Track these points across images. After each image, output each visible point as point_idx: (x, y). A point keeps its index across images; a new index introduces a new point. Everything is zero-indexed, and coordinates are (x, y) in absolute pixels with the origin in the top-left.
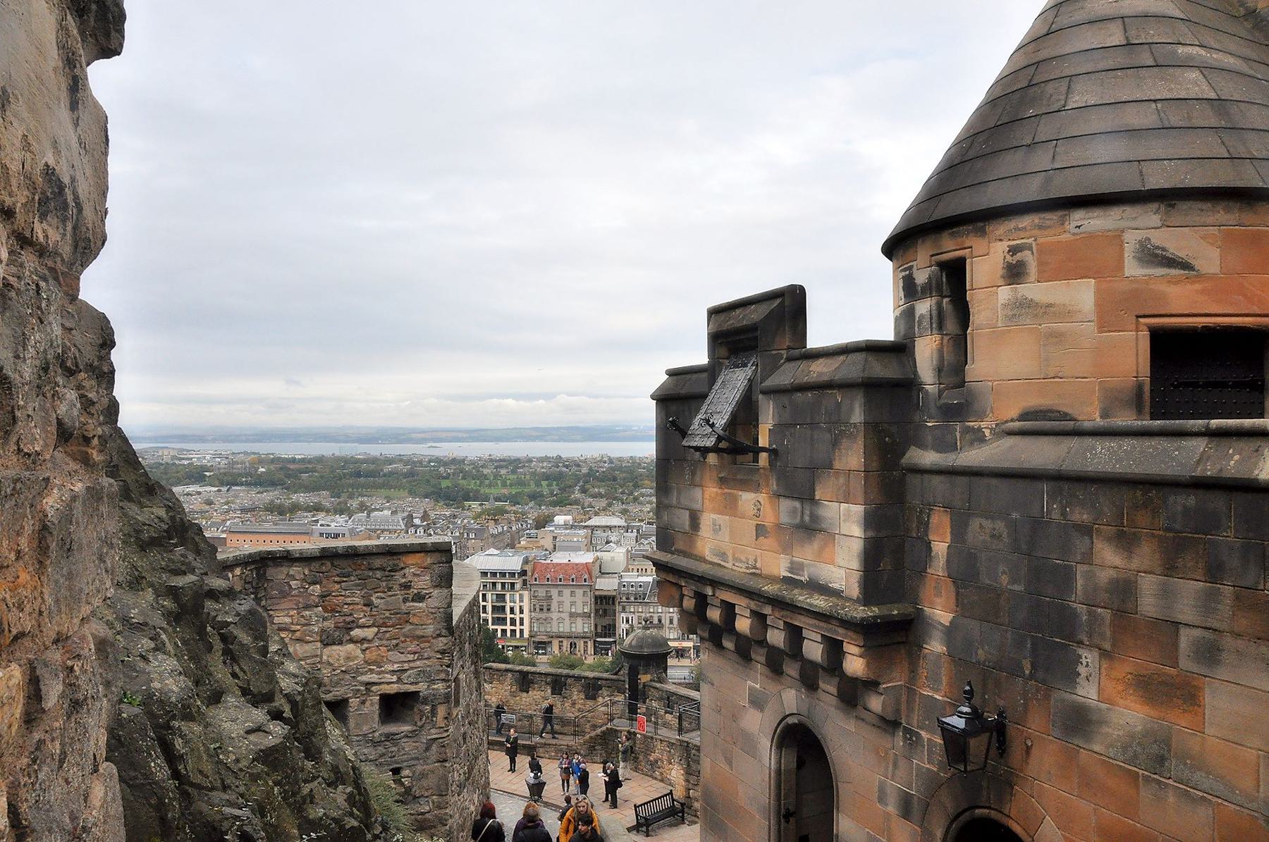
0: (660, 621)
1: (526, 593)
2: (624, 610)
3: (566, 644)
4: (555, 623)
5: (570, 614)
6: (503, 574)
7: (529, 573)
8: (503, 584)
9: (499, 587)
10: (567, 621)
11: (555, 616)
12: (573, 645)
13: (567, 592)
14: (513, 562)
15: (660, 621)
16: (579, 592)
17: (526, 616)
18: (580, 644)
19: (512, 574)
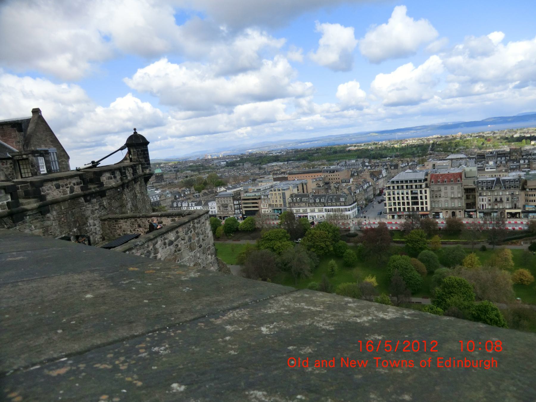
0: (501, 199)
1: (428, 190)
2: (480, 195)
3: (450, 212)
4: (443, 204)
5: (451, 198)
6: (416, 181)
7: (429, 180)
8: (416, 186)
9: (414, 187)
10: (450, 202)
11: (442, 199)
12: (454, 214)
13: (449, 187)
14: (421, 176)
15: (501, 199)
16: (456, 187)
17: (428, 200)
18: (457, 212)
19: (420, 181)
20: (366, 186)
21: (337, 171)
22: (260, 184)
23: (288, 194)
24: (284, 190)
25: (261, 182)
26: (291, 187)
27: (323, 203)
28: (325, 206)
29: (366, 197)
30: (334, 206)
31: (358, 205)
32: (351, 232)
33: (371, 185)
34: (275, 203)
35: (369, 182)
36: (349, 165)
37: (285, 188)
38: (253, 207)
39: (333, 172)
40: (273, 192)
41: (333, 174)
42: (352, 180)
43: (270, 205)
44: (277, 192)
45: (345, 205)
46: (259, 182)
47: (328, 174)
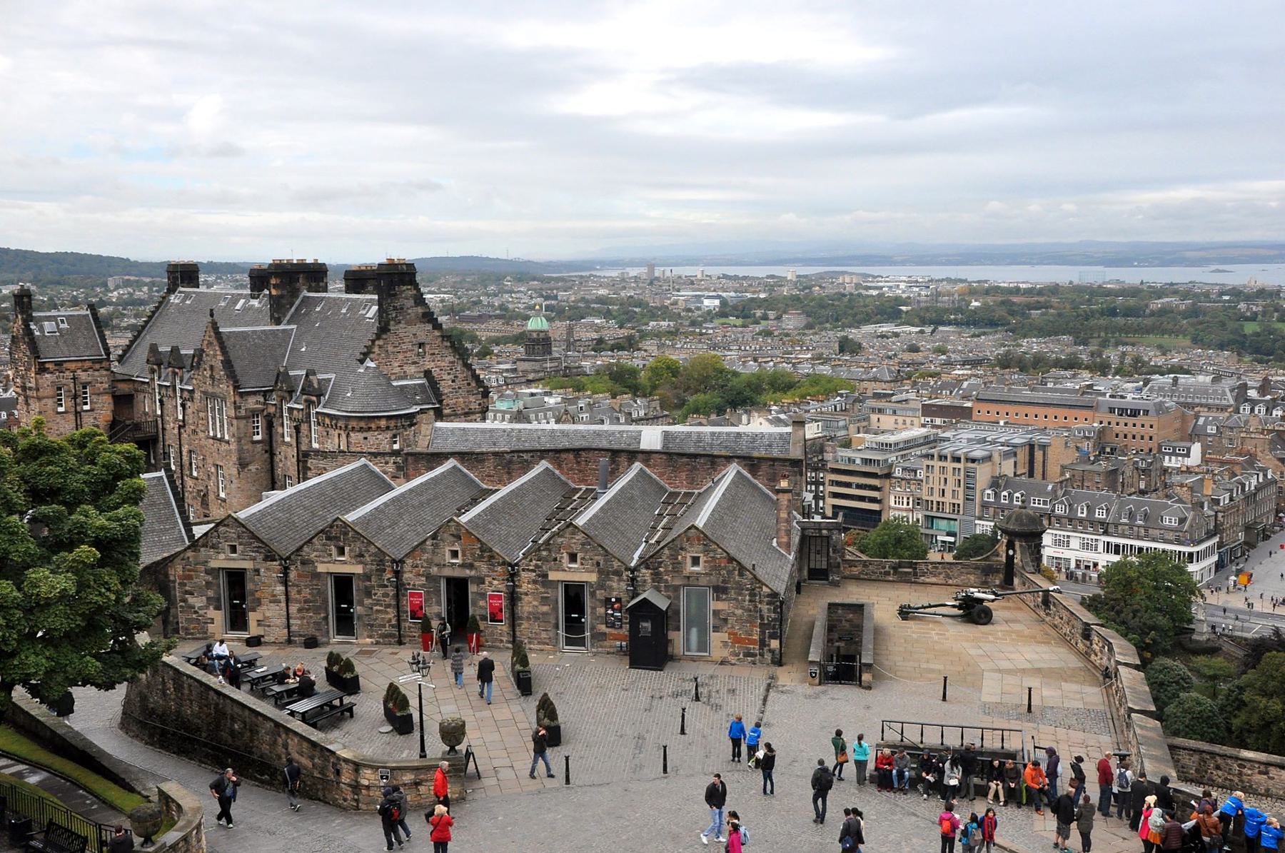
20: (1254, 482)
21: (1146, 412)
22: (874, 417)
23: (983, 475)
24: (973, 461)
25: (880, 411)
26: (996, 457)
27: (1102, 523)
28: (1106, 533)
29: (1250, 518)
30: (1138, 538)
31: (1220, 545)
32: (1195, 637)
33: (1275, 482)
34: (936, 498)
35: (1264, 471)
36: (1187, 390)
37: (978, 453)
38: (862, 499)
39: (1135, 413)
40: (937, 464)
41: (1131, 420)
42: (1196, 449)
43: (918, 501)
44: (950, 465)
45: (1180, 543)
46: (873, 410)
47: (1114, 418)
